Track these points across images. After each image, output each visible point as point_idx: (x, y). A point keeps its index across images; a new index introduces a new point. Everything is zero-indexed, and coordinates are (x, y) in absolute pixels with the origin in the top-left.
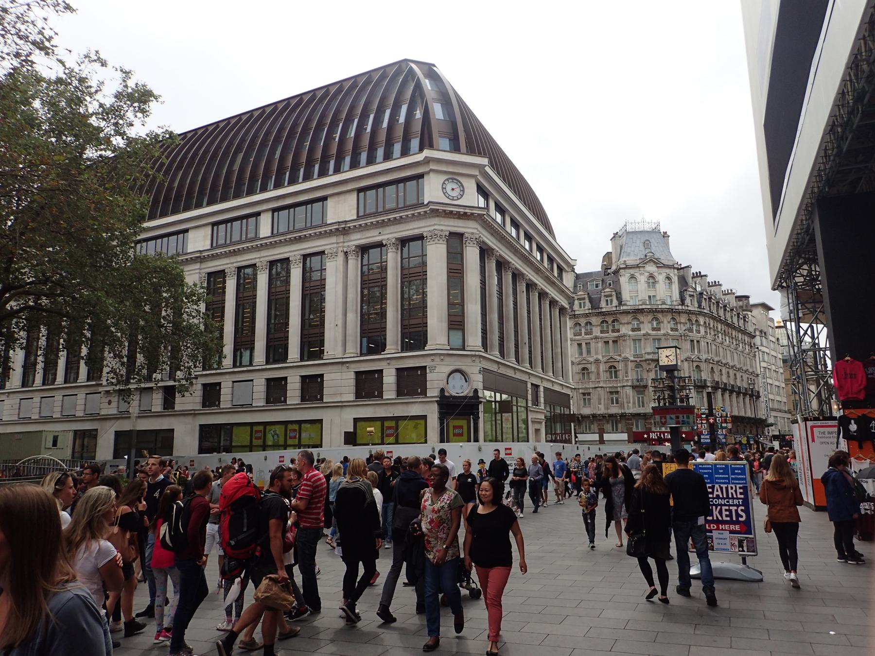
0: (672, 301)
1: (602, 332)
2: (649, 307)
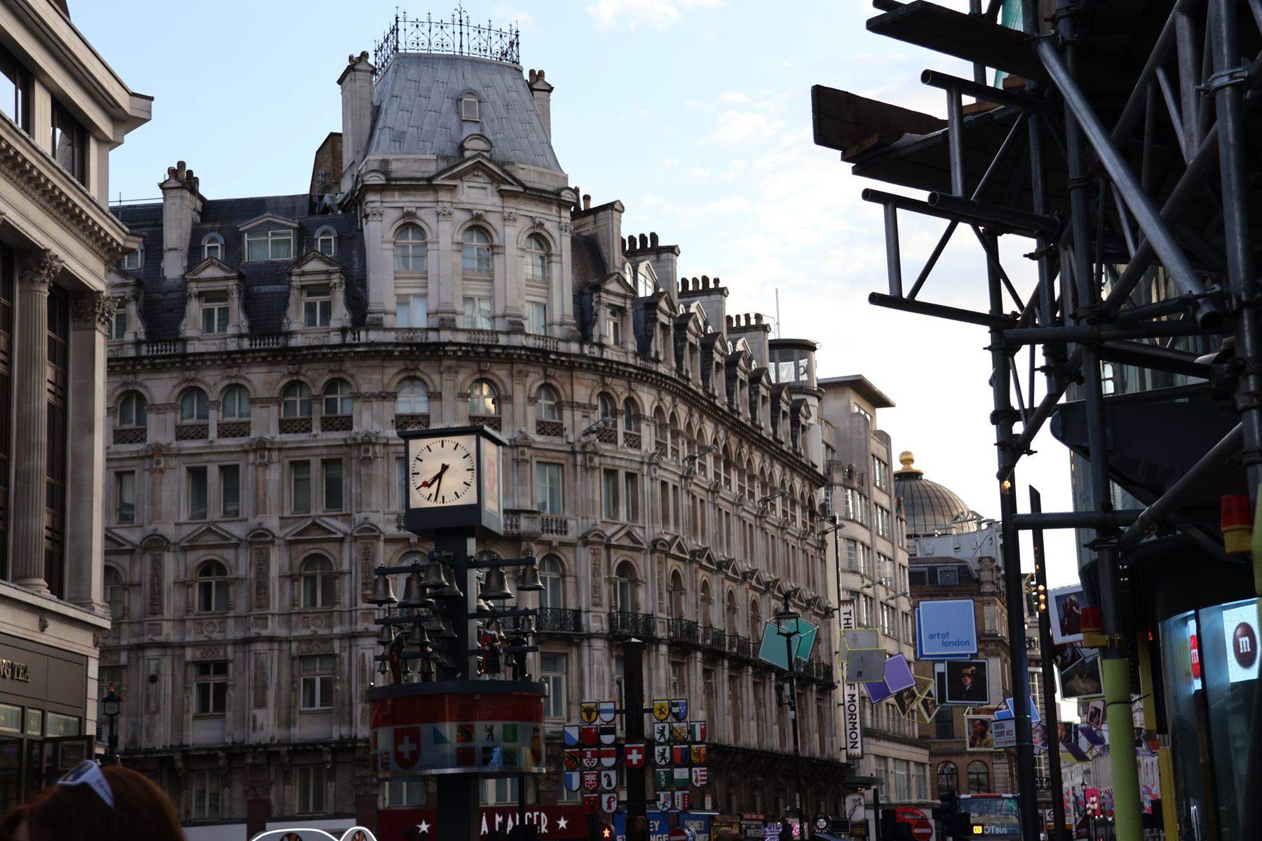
0: (548, 325)
1: (285, 426)
2: (462, 338)
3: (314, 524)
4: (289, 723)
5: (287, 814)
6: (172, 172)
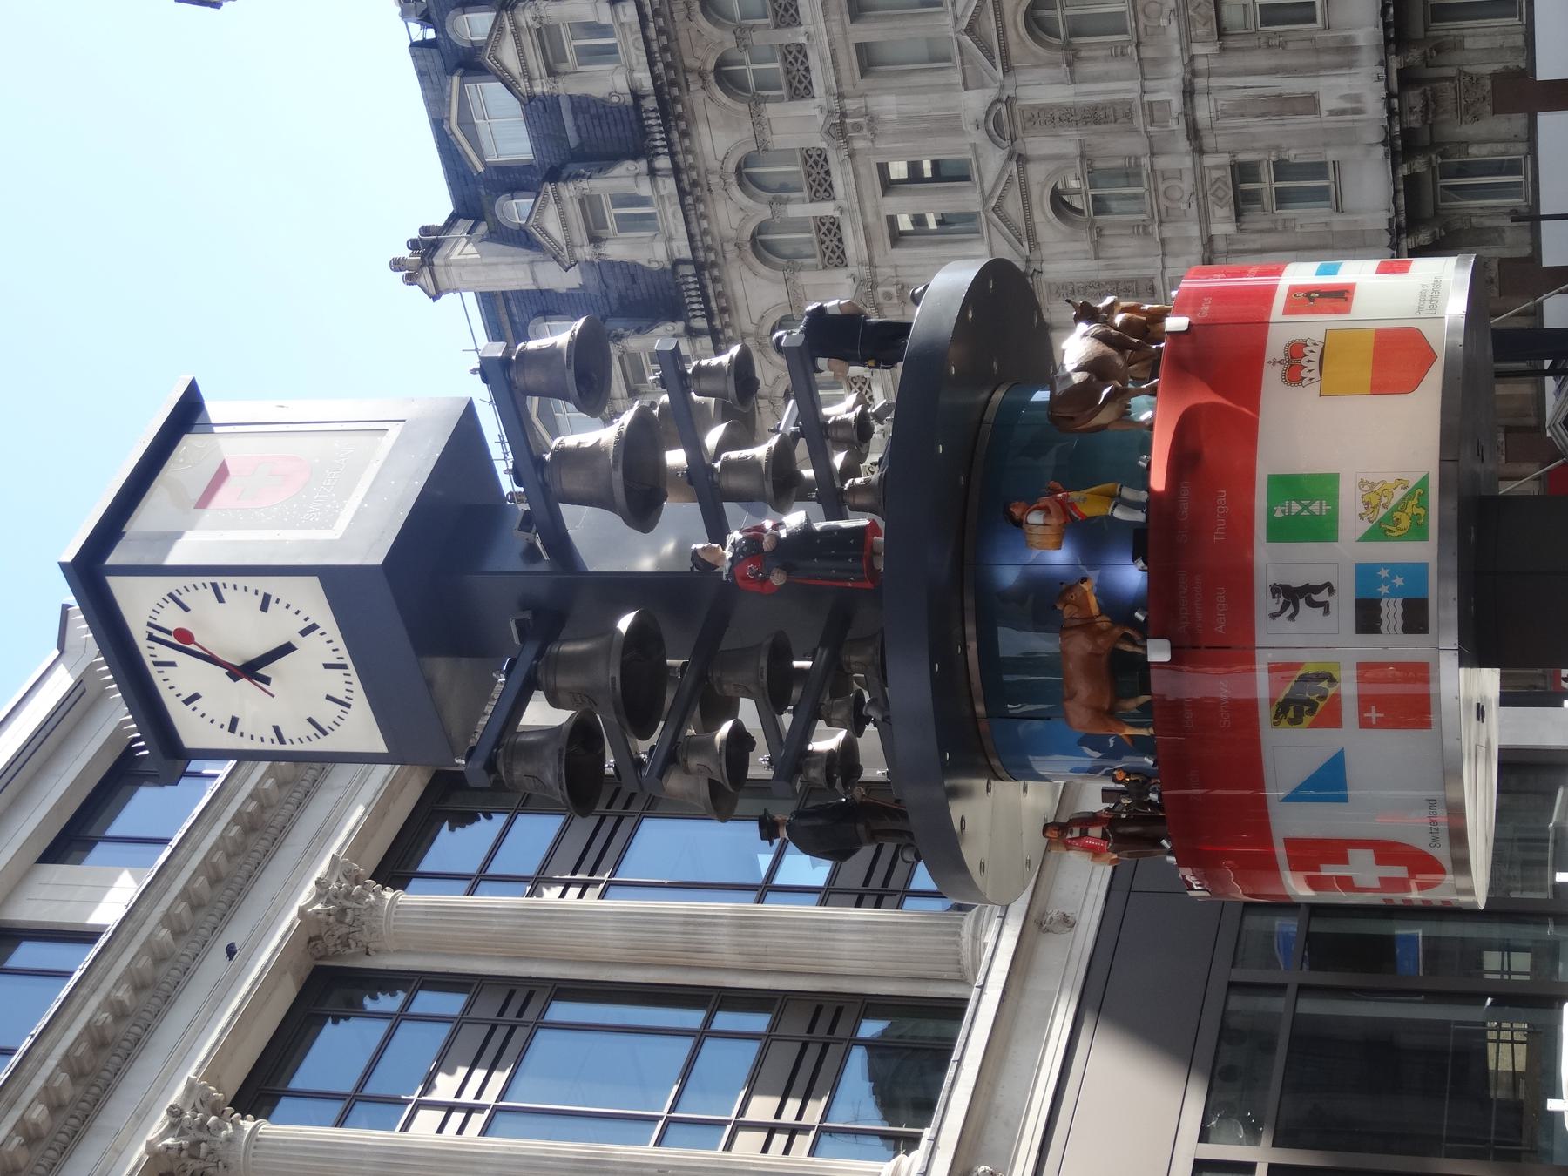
1: (800, 89)
3: (970, 30)
4: (1346, 52)
5: (1519, 41)
6: (410, 279)
